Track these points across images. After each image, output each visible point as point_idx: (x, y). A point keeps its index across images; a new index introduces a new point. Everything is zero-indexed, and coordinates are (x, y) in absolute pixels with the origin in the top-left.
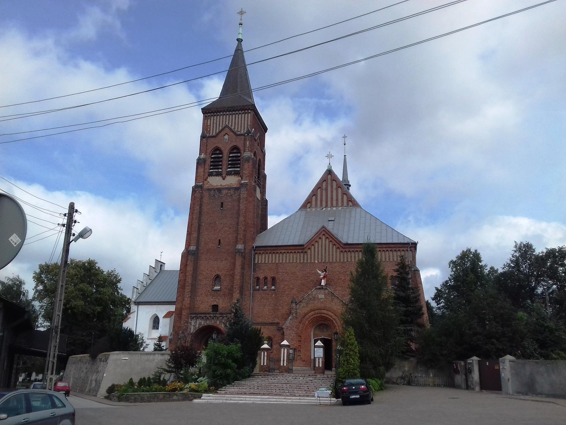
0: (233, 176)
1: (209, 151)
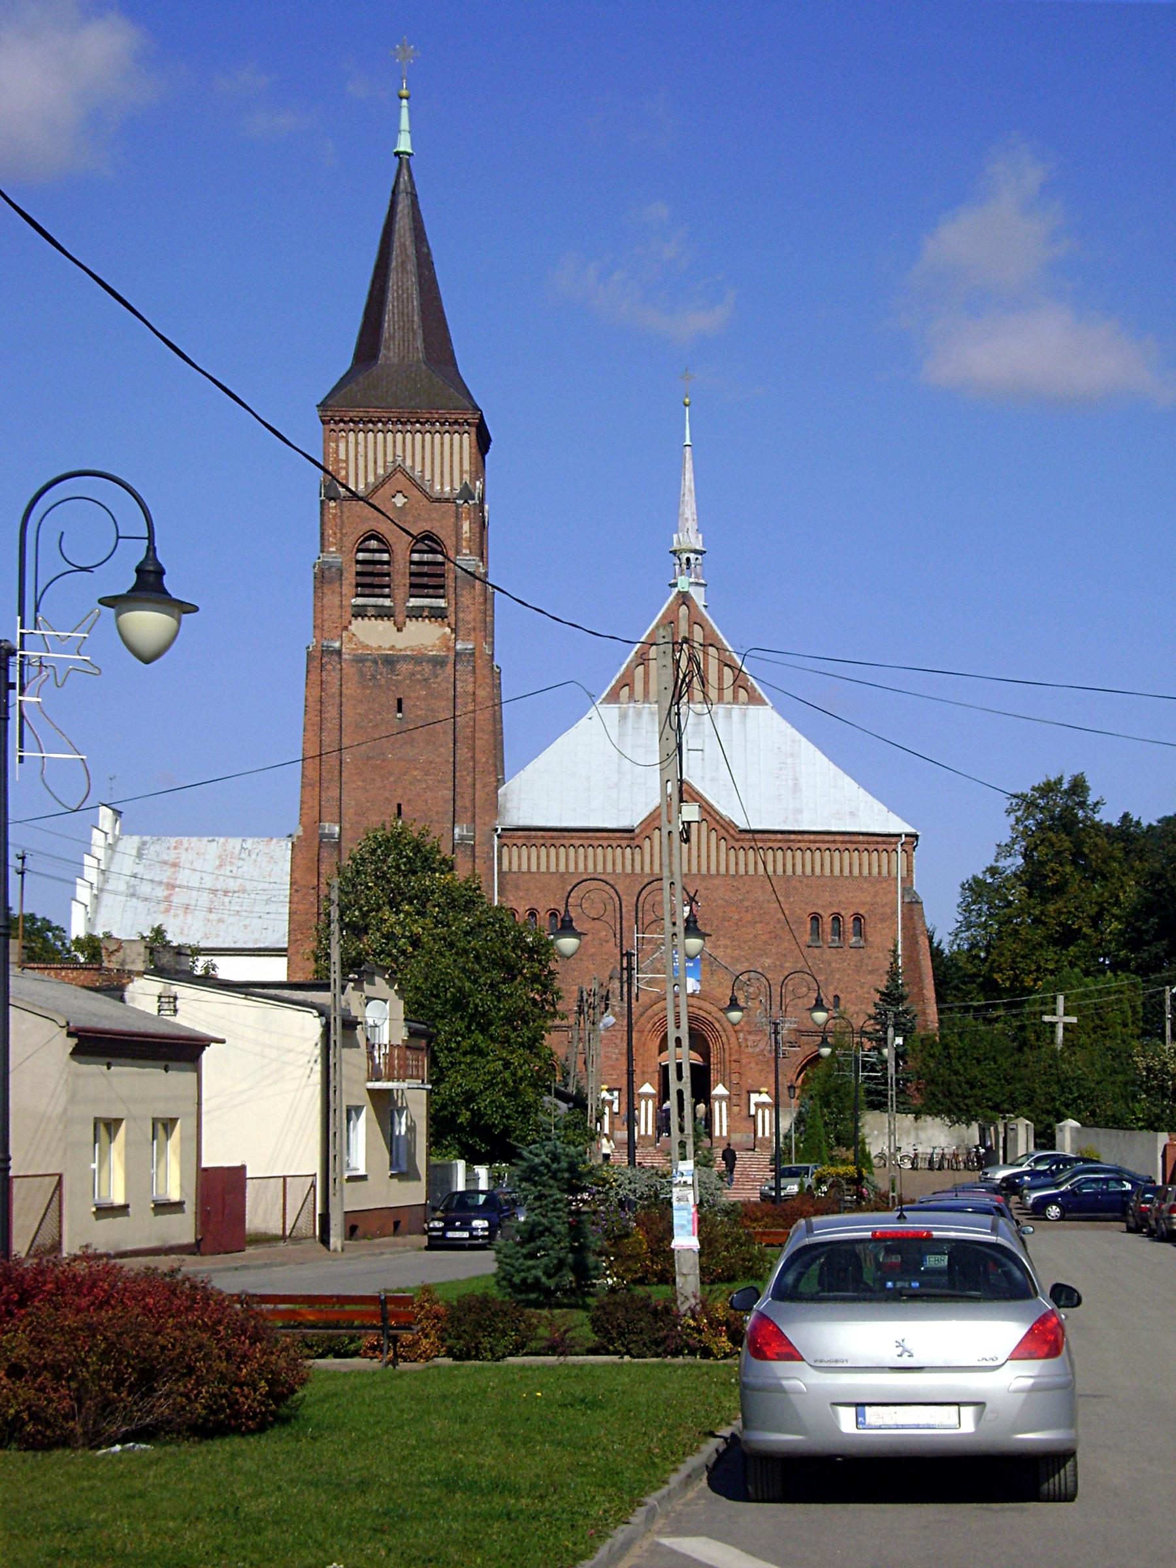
0: (427, 621)
1: (350, 541)
